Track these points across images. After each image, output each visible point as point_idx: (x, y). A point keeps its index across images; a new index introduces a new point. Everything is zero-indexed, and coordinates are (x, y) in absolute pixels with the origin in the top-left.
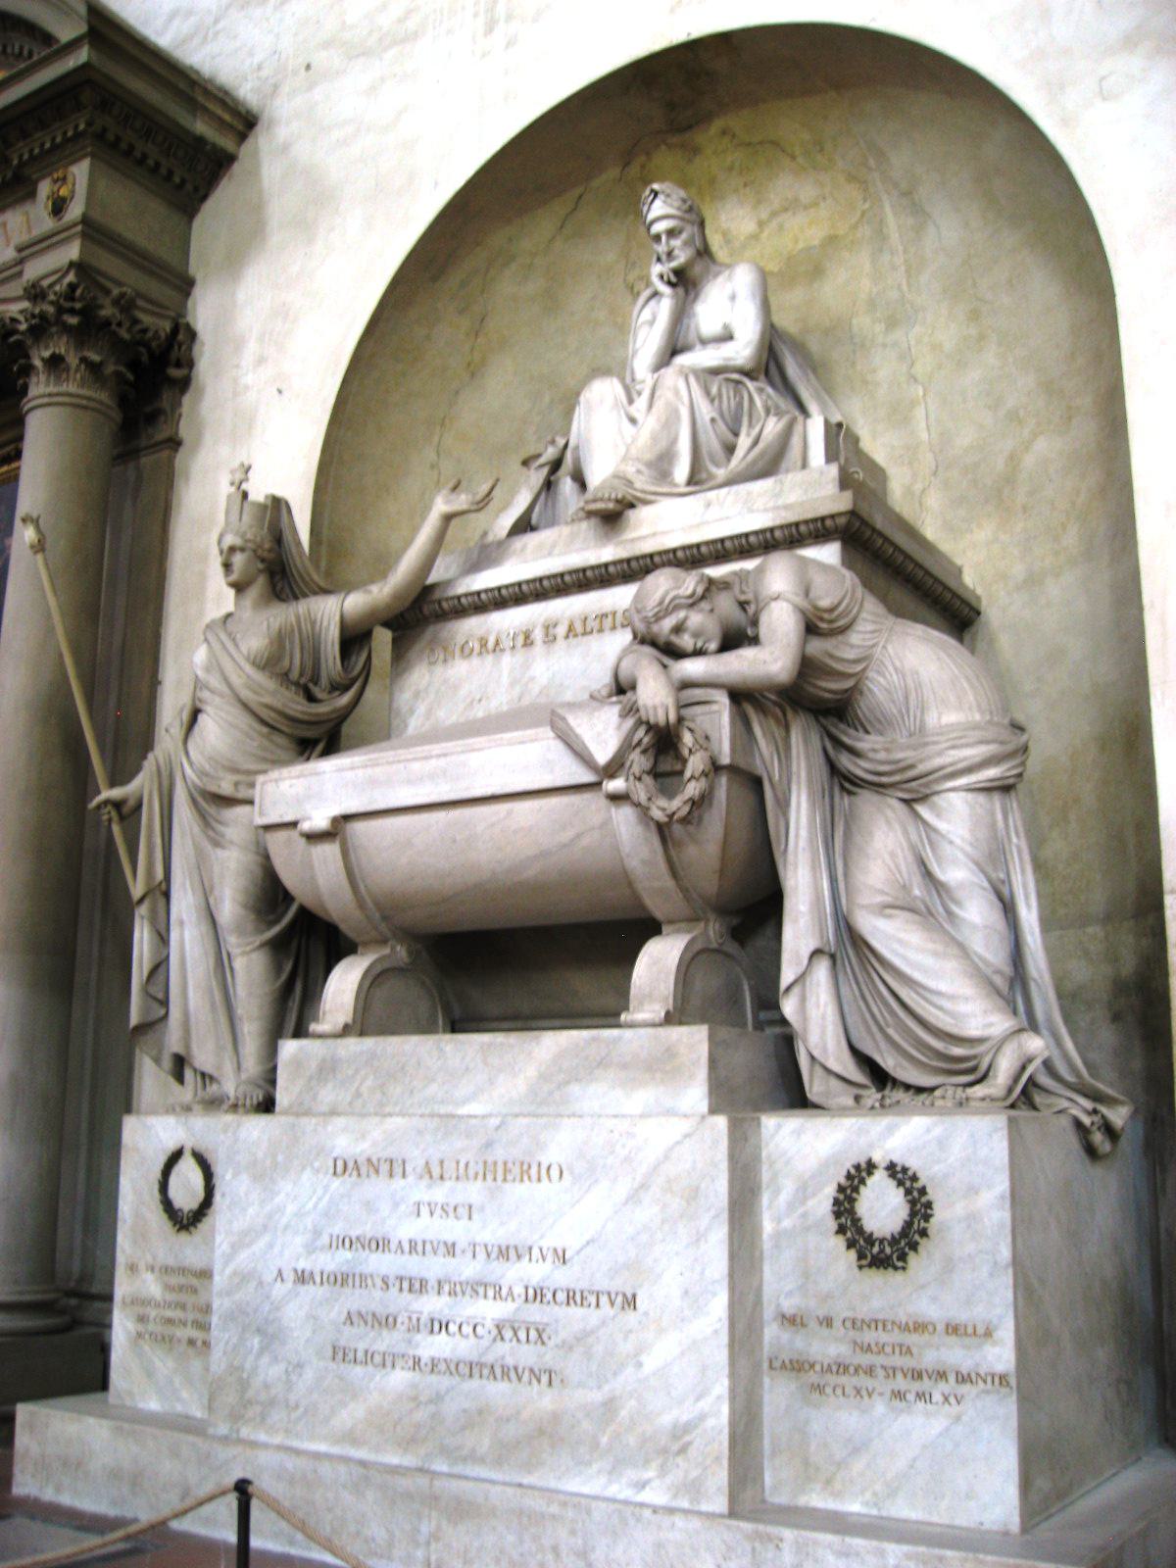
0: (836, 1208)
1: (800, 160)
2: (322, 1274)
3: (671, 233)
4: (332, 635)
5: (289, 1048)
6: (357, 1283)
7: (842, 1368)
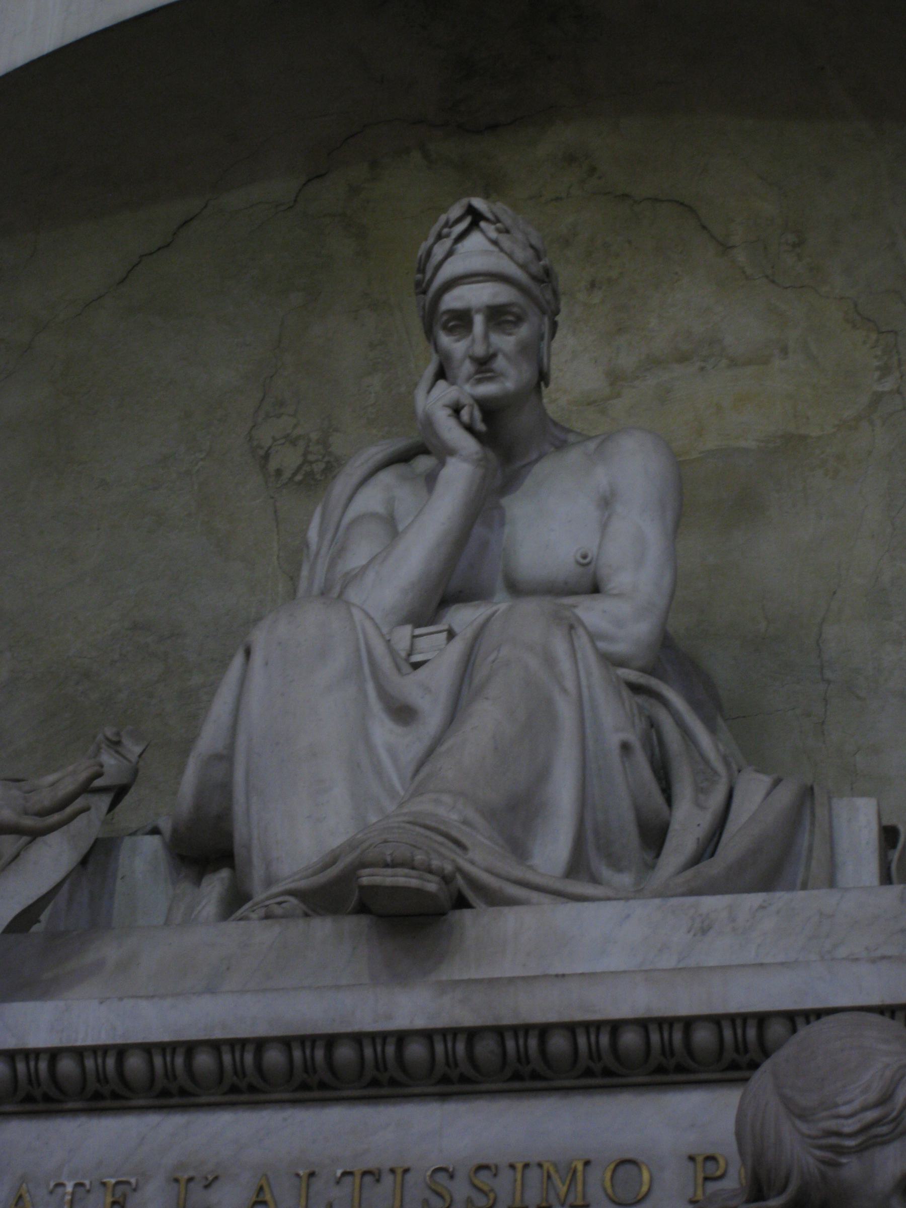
1: (741, 257)
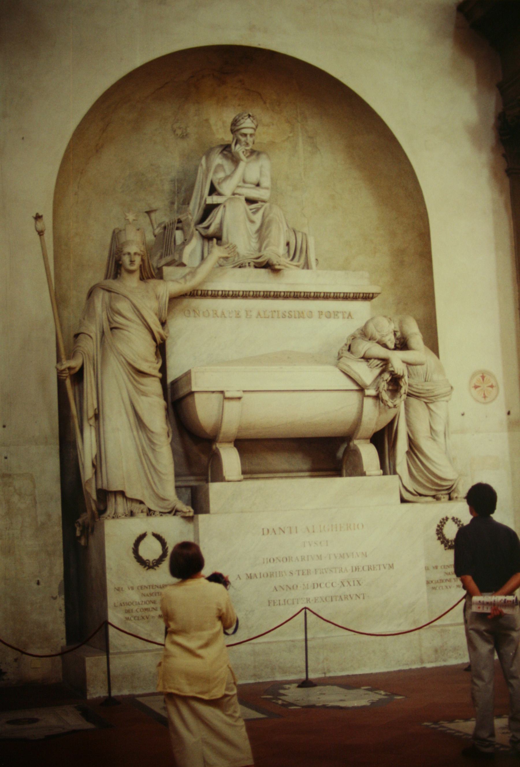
0: (437, 532)
1: (268, 105)
2: (260, 574)
3: (251, 135)
4: (165, 299)
5: (214, 488)
6: (278, 575)
7: (442, 581)
